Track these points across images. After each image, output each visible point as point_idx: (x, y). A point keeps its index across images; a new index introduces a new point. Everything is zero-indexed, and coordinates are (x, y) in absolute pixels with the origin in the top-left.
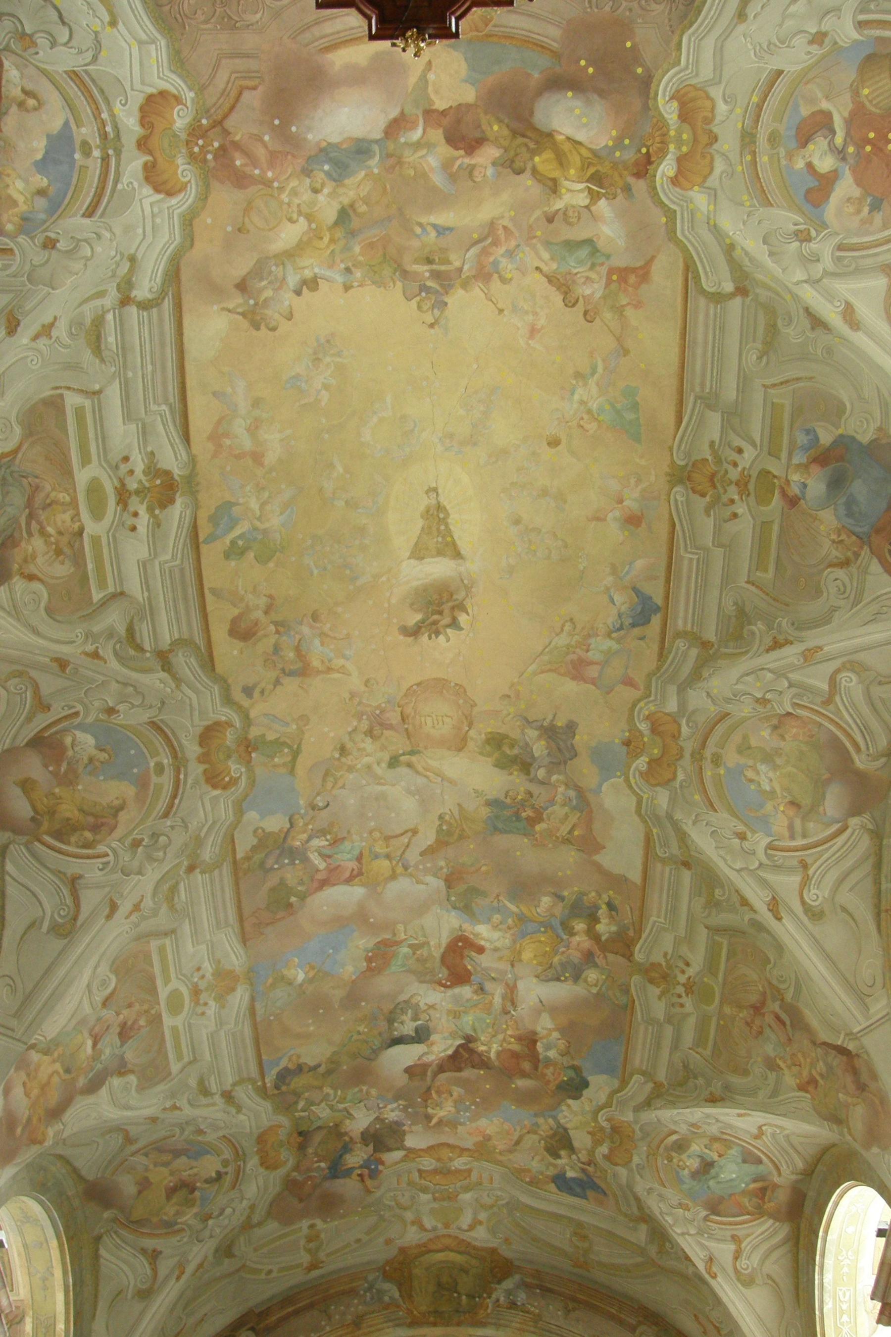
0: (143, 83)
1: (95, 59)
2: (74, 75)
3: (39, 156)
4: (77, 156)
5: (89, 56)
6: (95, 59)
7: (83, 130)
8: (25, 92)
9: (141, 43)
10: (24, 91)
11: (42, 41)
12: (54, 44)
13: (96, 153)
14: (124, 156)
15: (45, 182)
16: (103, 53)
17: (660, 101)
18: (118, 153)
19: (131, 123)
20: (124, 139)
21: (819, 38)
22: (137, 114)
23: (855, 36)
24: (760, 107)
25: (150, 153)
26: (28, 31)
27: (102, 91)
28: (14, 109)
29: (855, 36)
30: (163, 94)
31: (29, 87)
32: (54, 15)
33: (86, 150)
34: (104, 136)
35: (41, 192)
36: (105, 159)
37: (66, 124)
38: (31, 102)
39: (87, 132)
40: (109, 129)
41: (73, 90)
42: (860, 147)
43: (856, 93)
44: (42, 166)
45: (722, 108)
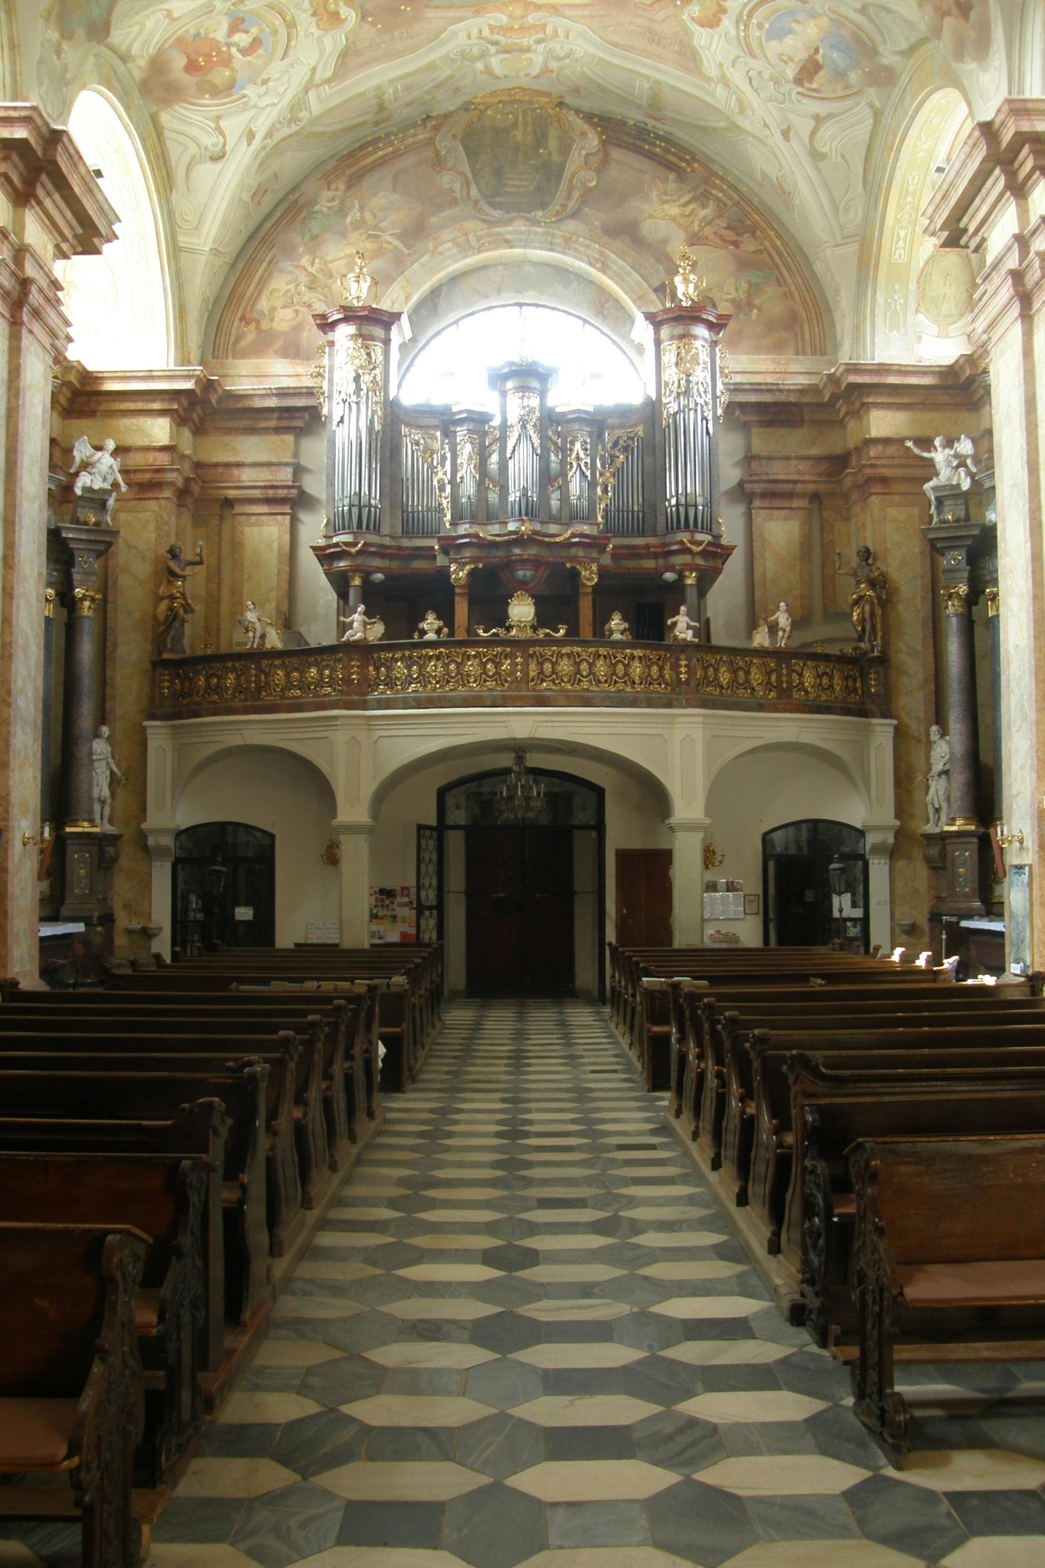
0: (713, 36)
1: (738, 57)
2: (752, 55)
3: (790, 36)
4: (767, 26)
5: (741, 60)
6: (738, 57)
7: (758, 34)
8: (787, 63)
9: (709, 50)
10: (787, 63)
11: (766, 76)
12: (760, 73)
13: (754, 21)
14: (738, 11)
15: (793, 25)
16: (732, 57)
17: (354, 15)
18: (740, 14)
19: (727, 23)
20: (734, 18)
21: (265, 82)
22: (721, 24)
23: (244, 92)
24: (289, 40)
25: (720, 5)
26: (772, 84)
27: (740, 43)
28: (796, 59)
29: (244, 92)
30: (703, 26)
31: (782, 64)
32: (753, 83)
33: (760, 26)
34: (747, 26)
35: (797, 22)
36: (750, 15)
37: (767, 41)
38: (785, 58)
39: (756, 33)
40: (742, 28)
41: (757, 51)
42: (219, 52)
43: (233, 70)
44: (790, 31)
45: (313, 29)
